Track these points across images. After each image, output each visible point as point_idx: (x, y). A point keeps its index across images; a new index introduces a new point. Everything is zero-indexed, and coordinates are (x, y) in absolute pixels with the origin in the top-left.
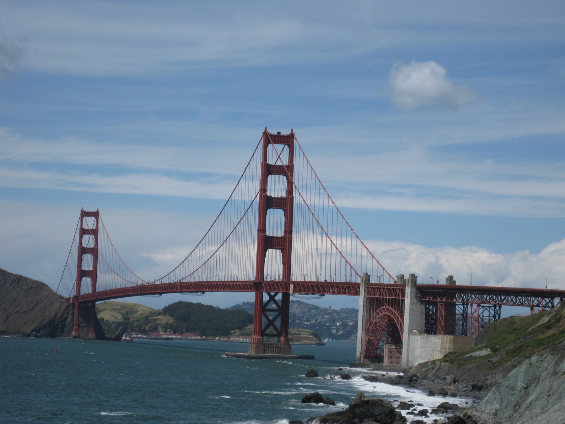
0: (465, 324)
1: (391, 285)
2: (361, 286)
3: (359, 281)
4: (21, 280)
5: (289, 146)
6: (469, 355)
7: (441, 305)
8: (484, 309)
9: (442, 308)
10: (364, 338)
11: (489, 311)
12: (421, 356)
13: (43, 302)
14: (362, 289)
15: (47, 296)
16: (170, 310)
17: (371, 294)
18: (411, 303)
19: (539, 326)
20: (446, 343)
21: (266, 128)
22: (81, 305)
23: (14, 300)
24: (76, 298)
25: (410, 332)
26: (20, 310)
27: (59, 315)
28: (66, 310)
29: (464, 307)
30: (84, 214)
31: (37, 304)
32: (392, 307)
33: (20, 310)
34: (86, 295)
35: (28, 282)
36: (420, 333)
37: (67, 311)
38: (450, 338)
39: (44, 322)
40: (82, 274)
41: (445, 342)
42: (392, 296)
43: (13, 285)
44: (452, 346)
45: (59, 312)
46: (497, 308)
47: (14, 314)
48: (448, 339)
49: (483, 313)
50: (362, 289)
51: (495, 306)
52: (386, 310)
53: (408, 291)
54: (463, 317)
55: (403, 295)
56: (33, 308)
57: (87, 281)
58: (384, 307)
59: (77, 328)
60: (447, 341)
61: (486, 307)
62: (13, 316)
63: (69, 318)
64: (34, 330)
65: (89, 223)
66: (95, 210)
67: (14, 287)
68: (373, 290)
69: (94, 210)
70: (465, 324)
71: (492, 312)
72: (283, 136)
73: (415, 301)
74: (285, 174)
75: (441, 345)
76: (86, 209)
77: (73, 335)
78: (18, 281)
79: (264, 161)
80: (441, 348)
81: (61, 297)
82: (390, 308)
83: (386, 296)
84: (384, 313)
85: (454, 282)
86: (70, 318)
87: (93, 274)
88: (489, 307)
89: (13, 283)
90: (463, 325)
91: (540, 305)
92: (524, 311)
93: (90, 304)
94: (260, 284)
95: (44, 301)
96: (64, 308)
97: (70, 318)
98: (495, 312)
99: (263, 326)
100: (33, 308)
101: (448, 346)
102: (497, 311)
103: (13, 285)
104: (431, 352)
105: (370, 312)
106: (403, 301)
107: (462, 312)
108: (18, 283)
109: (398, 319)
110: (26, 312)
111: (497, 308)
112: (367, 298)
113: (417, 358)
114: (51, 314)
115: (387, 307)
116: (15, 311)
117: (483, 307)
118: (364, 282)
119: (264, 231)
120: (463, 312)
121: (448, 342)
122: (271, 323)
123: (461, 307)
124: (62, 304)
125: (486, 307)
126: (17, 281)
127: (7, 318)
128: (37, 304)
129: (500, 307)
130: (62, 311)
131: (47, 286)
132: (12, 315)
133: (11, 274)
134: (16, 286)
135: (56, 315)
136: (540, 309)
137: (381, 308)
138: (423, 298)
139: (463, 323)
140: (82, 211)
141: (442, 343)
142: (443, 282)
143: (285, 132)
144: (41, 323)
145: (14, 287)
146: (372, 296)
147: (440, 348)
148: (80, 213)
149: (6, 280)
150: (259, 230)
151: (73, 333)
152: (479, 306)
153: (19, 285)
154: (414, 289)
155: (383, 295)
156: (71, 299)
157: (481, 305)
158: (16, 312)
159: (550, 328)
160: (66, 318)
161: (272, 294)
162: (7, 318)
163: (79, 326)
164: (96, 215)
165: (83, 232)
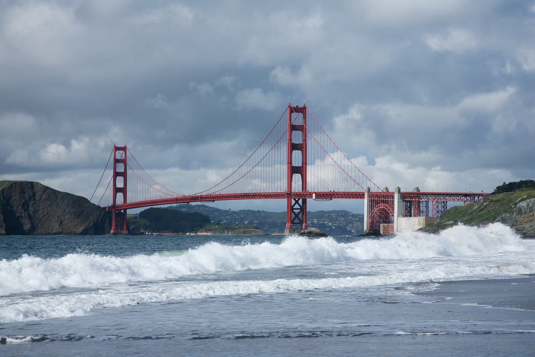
0: (427, 211)
1: (380, 193)
2: (365, 194)
3: (364, 191)
4: (68, 196)
5: (303, 113)
6: (444, 223)
7: (415, 202)
8: (439, 204)
9: (416, 204)
10: (368, 221)
11: (441, 205)
12: (405, 228)
14: (366, 195)
16: (142, 214)
17: (371, 198)
18: (398, 202)
19: (474, 210)
20: (421, 220)
21: (290, 104)
22: (116, 212)
23: (65, 210)
25: (398, 216)
26: (70, 217)
27: (100, 219)
29: (426, 203)
30: (117, 149)
32: (385, 204)
33: (70, 217)
34: (120, 206)
35: (73, 197)
36: (404, 217)
37: (105, 216)
38: (423, 218)
39: (90, 225)
40: (117, 190)
41: (420, 220)
42: (386, 198)
43: (62, 200)
44: (424, 222)
46: (445, 203)
47: (66, 220)
48: (422, 219)
49: (441, 205)
50: (366, 195)
51: (444, 202)
52: (382, 205)
53: (396, 196)
54: (426, 208)
55: (393, 198)
57: (120, 196)
58: (381, 204)
59: (115, 228)
60: (421, 219)
61: (440, 203)
63: (106, 221)
64: (83, 231)
65: (119, 155)
66: (124, 146)
67: (63, 201)
68: (373, 196)
69: (124, 146)
70: (427, 211)
71: (443, 205)
72: (300, 108)
73: (401, 200)
74: (300, 130)
75: (418, 222)
76: (119, 145)
77: (112, 233)
78: (66, 196)
79: (290, 123)
80: (418, 223)
81: (99, 207)
82: (385, 205)
83: (382, 198)
84: (381, 207)
85: (419, 190)
86: (107, 221)
87: (123, 190)
88: (442, 202)
89: (62, 198)
90: (426, 212)
91: (468, 200)
92: (460, 204)
93: (122, 211)
94: (290, 194)
95: (86, 210)
96: (102, 214)
98: (444, 205)
99: (292, 218)
100: (79, 216)
101: (422, 222)
102: (445, 204)
103: (62, 200)
104: (412, 225)
105: (372, 207)
106: (393, 201)
107: (425, 205)
108: (66, 198)
109: (390, 210)
111: (445, 203)
112: (369, 200)
113: (403, 229)
115: (383, 204)
116: (66, 219)
117: (438, 202)
118: (367, 192)
119: (291, 163)
120: (426, 205)
121: (422, 220)
122: (297, 216)
123: (425, 202)
124: (100, 212)
125: (440, 203)
126: (65, 197)
127: (61, 223)
128: (82, 213)
129: (447, 202)
130: (102, 216)
131: (87, 199)
132: (64, 220)
133: (59, 192)
134: (65, 201)
135: (98, 218)
136: (469, 202)
137: (379, 205)
138: (404, 199)
139: (426, 211)
140: (115, 147)
141: (419, 221)
142: (415, 191)
143: (301, 106)
144: (88, 225)
145: (63, 201)
146: (373, 199)
147: (418, 223)
148: (113, 147)
150: (288, 163)
151: (112, 231)
152: (437, 202)
153: (67, 199)
154: (400, 195)
155: (380, 198)
156: (107, 208)
157: (438, 201)
159: (483, 210)
161: (297, 199)
162: (61, 223)
163: (116, 226)
164: (124, 149)
165: (117, 161)
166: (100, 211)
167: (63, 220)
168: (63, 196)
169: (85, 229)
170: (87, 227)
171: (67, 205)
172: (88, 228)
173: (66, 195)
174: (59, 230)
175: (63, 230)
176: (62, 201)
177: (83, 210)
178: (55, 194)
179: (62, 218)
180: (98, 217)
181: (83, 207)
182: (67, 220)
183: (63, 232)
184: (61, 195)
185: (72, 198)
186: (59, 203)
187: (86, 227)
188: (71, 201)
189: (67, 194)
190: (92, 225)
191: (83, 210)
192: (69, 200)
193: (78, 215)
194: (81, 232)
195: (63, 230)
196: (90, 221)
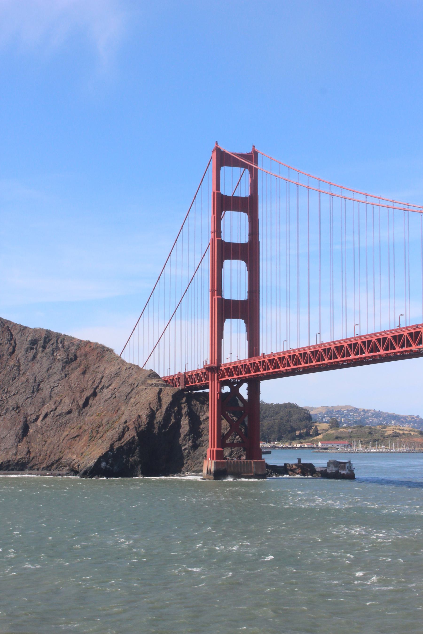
13: (108, 387)
15: (117, 374)
23: (39, 385)
24: (210, 370)
27: (159, 417)
28: (172, 404)
31: (95, 394)
39: (127, 437)
43: (32, 353)
45: (157, 410)
47: (41, 418)
56: (86, 404)
62: (39, 423)
67: (34, 357)
76: (228, 149)
81: (153, 375)
86: (185, 422)
89: (32, 349)
96: (167, 400)
97: (185, 422)
100: (86, 404)
103: (32, 353)
108: (44, 347)
110: (69, 412)
114: (139, 416)
116: (44, 413)
126: (41, 343)
127: (26, 429)
128: (95, 394)
130: (164, 407)
132: (36, 420)
133: (24, 329)
134: (39, 355)
135: (152, 415)
144: (119, 439)
145: (34, 357)
149: (15, 343)
153: (47, 350)
158: (46, 415)
160: (177, 425)
162: (26, 429)
166: (157, 389)
167: (33, 417)
168: (34, 342)
169: (106, 453)
170: (115, 447)
171: (48, 370)
172: (118, 449)
173: (43, 336)
174: (16, 454)
175: (32, 455)
176: (30, 358)
177: (100, 387)
178: (12, 335)
179: (30, 410)
180: (152, 410)
181: (100, 376)
182: (47, 419)
183: (29, 462)
184: (29, 339)
185: (63, 347)
186: (22, 362)
187: (112, 446)
188: (59, 357)
189: (48, 332)
190: (134, 437)
191: (100, 387)
192: (53, 354)
193: (81, 403)
194: (91, 464)
195: (32, 455)
196: (126, 422)
